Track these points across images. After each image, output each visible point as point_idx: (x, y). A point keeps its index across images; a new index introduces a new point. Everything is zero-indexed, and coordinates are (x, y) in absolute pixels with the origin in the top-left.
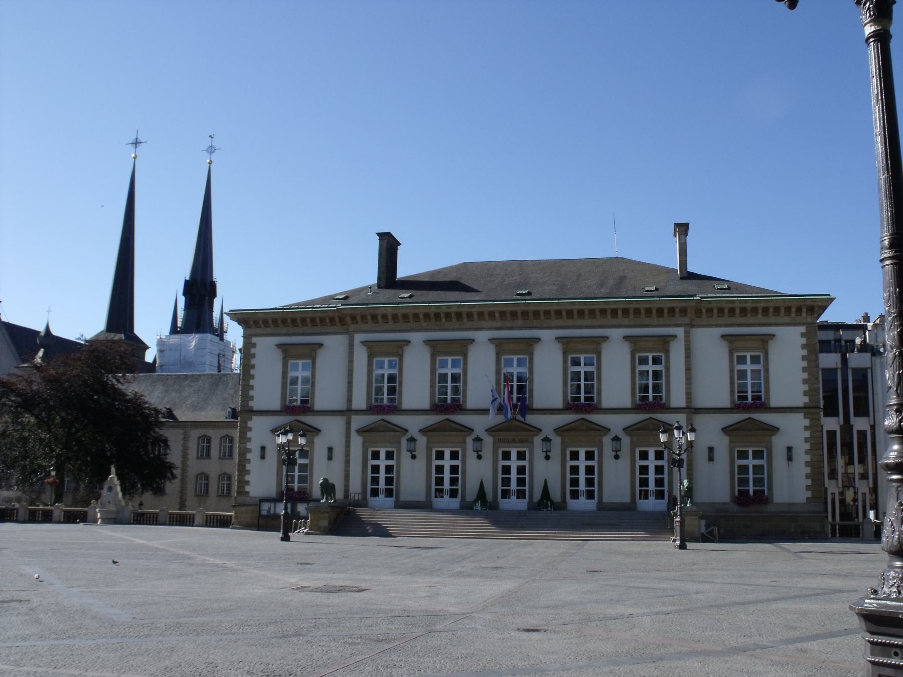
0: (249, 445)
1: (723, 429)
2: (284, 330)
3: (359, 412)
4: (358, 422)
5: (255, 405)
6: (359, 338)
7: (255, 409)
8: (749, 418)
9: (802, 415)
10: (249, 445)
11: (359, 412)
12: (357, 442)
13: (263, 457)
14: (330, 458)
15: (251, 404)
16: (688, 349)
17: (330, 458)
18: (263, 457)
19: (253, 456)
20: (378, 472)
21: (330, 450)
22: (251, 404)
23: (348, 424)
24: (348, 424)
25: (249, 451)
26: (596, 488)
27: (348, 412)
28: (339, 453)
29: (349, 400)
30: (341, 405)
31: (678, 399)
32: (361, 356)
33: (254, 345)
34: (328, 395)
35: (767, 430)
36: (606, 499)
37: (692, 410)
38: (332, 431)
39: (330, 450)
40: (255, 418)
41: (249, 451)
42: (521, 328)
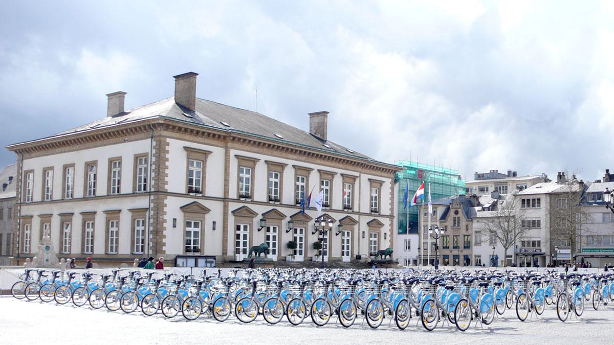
0: (165, 217)
1: (181, 208)
2: (187, 137)
3: (233, 200)
4: (233, 206)
5: (169, 188)
6: (233, 152)
7: (168, 191)
8: (195, 202)
9: (389, 219)
10: (165, 217)
11: (233, 200)
12: (231, 219)
13: (174, 226)
14: (214, 229)
15: (166, 187)
16: (360, 183)
17: (214, 229)
18: (174, 226)
19: (168, 225)
20: (239, 239)
21: (214, 223)
22: (166, 187)
23: (225, 207)
24: (225, 207)
25: (165, 221)
26: (328, 250)
27: (225, 200)
28: (219, 226)
29: (226, 191)
30: (222, 196)
31: (356, 209)
32: (234, 164)
33: (168, 144)
34: (213, 187)
35: (354, 222)
36: (333, 256)
37: (359, 213)
38: (215, 211)
39: (214, 223)
40: (168, 197)
41: (165, 221)
42: (305, 162)
